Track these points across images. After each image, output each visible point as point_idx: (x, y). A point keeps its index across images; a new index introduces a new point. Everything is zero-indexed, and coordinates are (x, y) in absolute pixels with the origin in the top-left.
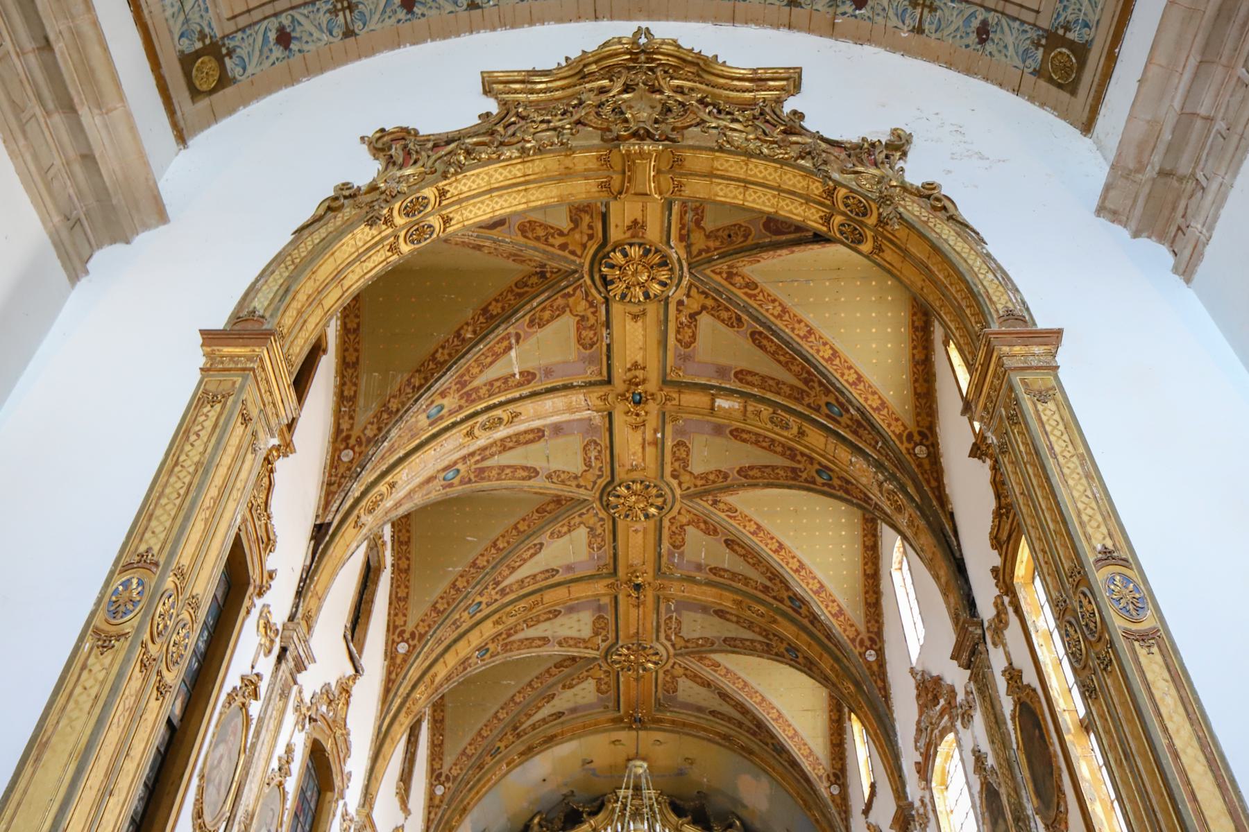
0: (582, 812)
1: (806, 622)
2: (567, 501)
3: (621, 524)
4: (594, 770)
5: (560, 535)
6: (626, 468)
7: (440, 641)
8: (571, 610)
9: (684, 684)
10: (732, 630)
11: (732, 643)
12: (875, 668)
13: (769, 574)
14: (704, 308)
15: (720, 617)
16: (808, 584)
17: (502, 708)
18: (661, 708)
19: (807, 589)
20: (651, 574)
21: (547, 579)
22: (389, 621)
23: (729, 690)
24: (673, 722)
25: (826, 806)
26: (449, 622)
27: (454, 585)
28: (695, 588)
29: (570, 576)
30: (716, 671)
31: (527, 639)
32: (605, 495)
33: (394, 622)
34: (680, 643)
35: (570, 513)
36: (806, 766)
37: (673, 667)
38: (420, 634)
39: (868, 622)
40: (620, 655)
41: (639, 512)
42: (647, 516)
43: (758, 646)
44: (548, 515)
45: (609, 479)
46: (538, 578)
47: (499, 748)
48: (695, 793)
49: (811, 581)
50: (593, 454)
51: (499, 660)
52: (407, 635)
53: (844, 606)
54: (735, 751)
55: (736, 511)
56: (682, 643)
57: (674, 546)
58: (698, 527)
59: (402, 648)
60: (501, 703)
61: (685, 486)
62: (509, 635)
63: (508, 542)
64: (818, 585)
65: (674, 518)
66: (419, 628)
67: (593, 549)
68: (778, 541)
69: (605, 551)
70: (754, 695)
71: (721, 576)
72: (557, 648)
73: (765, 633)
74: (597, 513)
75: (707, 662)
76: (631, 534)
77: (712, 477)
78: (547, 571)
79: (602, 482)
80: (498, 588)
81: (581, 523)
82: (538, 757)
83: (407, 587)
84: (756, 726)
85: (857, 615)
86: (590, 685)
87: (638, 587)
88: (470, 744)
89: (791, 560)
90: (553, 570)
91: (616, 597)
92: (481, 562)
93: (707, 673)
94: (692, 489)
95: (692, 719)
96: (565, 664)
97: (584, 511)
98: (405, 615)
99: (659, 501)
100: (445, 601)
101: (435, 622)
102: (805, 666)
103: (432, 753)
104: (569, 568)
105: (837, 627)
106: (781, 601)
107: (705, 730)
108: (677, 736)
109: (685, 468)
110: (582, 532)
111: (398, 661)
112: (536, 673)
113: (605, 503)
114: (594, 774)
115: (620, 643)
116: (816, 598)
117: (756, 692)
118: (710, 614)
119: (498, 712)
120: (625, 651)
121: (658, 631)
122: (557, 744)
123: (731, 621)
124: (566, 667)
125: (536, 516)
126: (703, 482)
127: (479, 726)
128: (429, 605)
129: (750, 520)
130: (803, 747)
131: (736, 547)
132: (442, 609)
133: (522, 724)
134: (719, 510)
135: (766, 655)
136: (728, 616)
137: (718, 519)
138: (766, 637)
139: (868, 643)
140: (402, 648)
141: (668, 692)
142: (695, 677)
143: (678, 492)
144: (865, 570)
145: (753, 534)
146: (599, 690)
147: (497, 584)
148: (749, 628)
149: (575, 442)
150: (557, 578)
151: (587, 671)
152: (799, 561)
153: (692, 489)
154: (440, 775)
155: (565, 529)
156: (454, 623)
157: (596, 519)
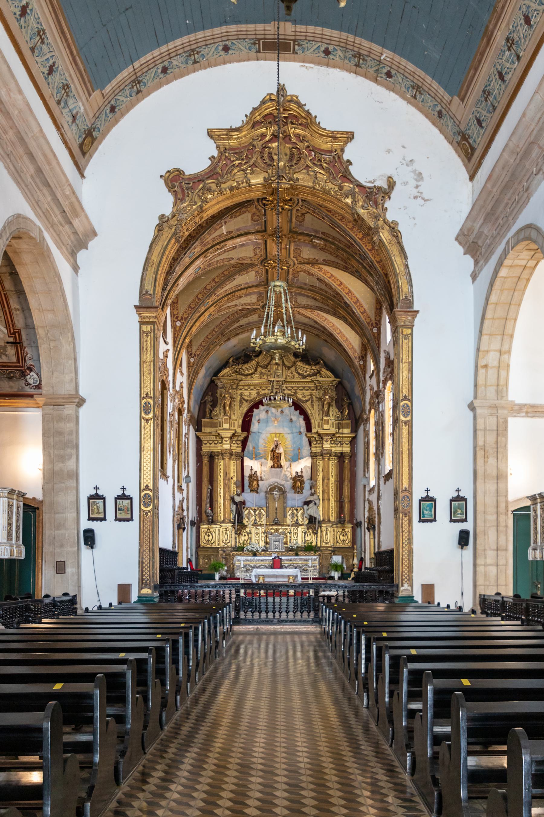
5: (243, 275)
10: (320, 305)
12: (376, 335)
14: (308, 212)
27: (197, 297)
50: (258, 251)
60: (216, 325)
85: (371, 312)
92: (209, 287)
105: (362, 318)
111: (177, 329)
125: (232, 269)
140: (178, 324)
143: (296, 262)
150: (241, 287)
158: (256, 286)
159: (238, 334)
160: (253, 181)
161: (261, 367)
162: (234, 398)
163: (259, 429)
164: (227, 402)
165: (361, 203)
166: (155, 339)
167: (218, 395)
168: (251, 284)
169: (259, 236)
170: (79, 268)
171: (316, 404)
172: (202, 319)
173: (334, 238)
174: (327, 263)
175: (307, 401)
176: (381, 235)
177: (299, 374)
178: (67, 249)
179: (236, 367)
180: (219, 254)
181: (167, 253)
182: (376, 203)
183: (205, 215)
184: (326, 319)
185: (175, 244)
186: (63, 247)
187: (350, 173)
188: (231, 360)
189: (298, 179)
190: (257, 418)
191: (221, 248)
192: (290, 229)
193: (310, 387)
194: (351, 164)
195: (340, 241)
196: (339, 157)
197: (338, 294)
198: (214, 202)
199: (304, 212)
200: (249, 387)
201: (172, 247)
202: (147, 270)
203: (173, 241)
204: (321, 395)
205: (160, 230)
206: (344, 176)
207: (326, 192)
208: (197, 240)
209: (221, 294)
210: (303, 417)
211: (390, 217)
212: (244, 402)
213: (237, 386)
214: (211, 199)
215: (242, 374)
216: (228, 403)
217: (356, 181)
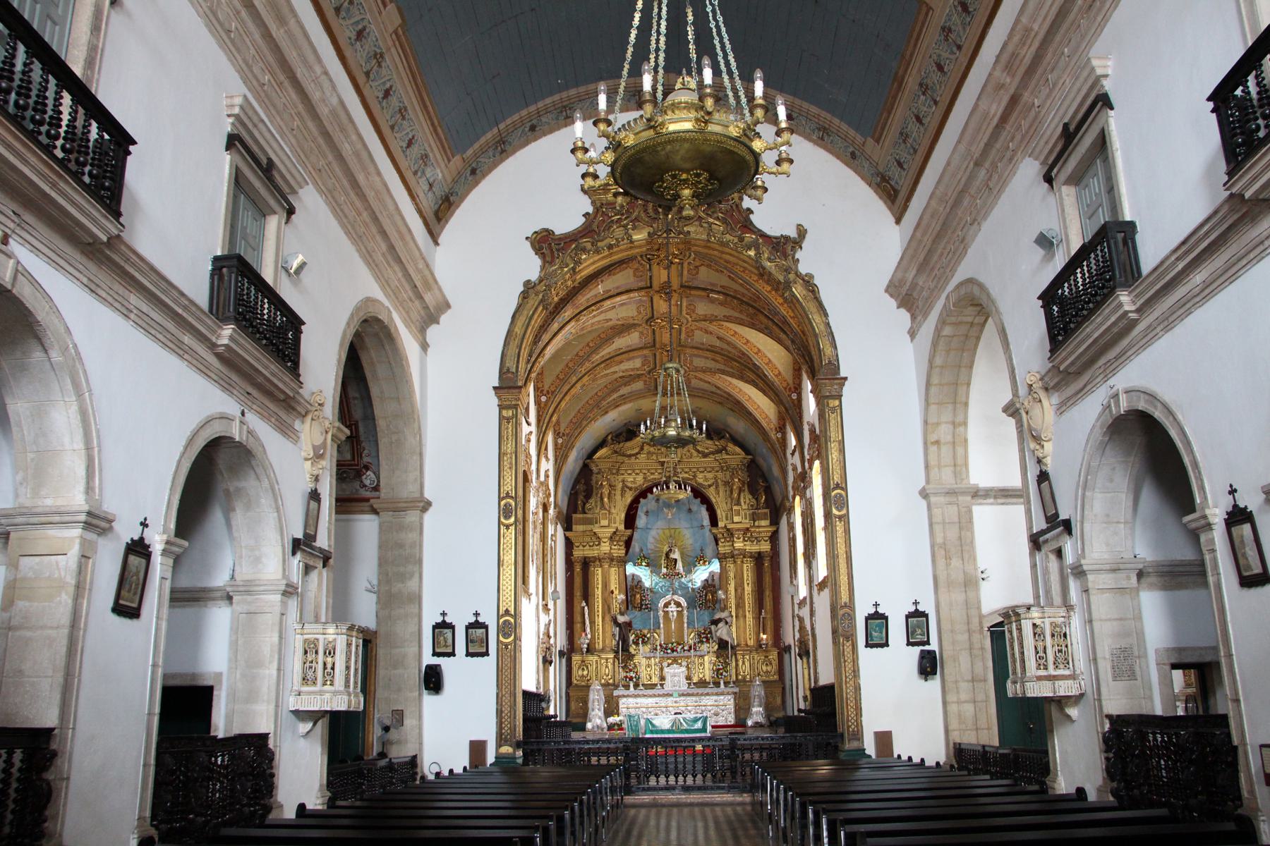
5: (623, 337)
10: (723, 367)
14: (702, 265)
27: (567, 365)
34: (691, 367)
36: (764, 424)
52: (545, 392)
59: (543, 399)
60: (590, 395)
139: (793, 390)
140: (543, 399)
149: (634, 307)
150: (622, 351)
158: (641, 348)
159: (618, 406)
160: (635, 237)
162: (614, 486)
164: (606, 491)
165: (766, 256)
166: (517, 426)
167: (593, 482)
168: (633, 348)
169: (643, 293)
170: (429, 346)
171: (721, 489)
172: (573, 391)
173: (736, 291)
174: (728, 319)
175: (710, 486)
176: (794, 290)
177: (698, 451)
178: (416, 328)
179: (617, 447)
180: (594, 316)
181: (533, 322)
182: (785, 256)
183: (578, 277)
184: (731, 383)
185: (543, 310)
186: (412, 325)
187: (751, 223)
188: (609, 437)
189: (689, 232)
190: (645, 509)
191: (597, 309)
192: (682, 282)
193: (713, 468)
194: (752, 212)
195: (743, 295)
196: (737, 206)
197: (744, 354)
198: (588, 262)
199: (698, 264)
200: (634, 471)
201: (539, 316)
202: (509, 344)
203: (541, 308)
204: (728, 477)
205: (524, 298)
206: (745, 227)
207: (723, 244)
208: (568, 302)
209: (597, 360)
210: (705, 506)
211: (803, 269)
212: (628, 490)
213: (618, 470)
214: (585, 259)
215: (624, 455)
216: (606, 493)
217: (760, 230)
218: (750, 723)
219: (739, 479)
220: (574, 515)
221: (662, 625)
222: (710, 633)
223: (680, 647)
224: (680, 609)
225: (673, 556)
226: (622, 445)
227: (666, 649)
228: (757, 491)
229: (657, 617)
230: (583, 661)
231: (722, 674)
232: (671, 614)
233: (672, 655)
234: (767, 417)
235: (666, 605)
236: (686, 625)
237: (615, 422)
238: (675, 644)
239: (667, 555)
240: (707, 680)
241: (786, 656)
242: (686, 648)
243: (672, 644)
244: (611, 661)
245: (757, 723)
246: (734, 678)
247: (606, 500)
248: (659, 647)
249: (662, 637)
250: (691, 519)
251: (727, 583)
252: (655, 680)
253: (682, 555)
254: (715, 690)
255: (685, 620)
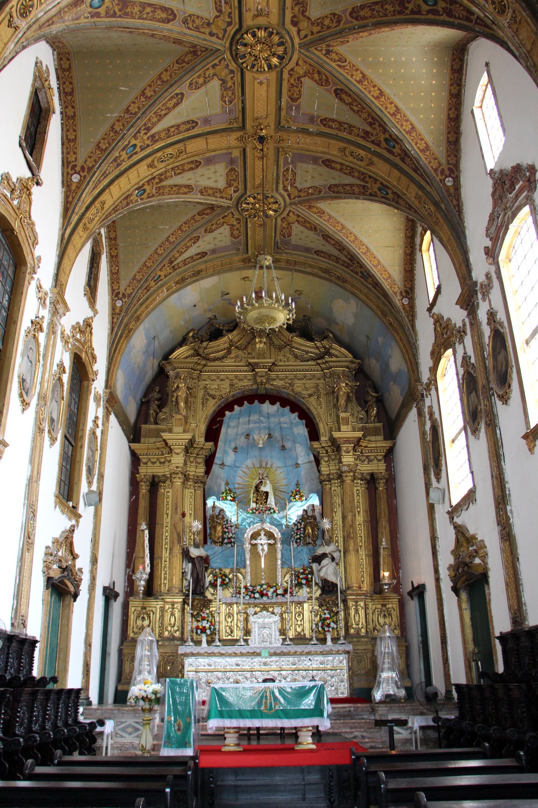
0: (222, 330)
1: (397, 160)
2: (202, 51)
3: (248, 76)
4: (230, 300)
6: (252, 14)
7: (105, 175)
8: (209, 161)
9: (296, 229)
11: (336, 189)
13: (370, 120)
15: (327, 166)
16: (402, 125)
17: (161, 246)
18: (279, 250)
19: (401, 130)
20: (273, 126)
21: (188, 130)
22: (63, 158)
23: (330, 232)
24: (287, 261)
25: (399, 312)
26: (111, 158)
27: (112, 128)
28: (309, 140)
29: (207, 129)
30: (321, 217)
31: (176, 186)
32: (234, 43)
33: (67, 158)
35: (204, 63)
36: (386, 285)
37: (288, 215)
38: (88, 167)
39: (449, 156)
40: (248, 204)
41: (263, 62)
42: (270, 67)
43: (356, 189)
44: (187, 66)
45: (237, 27)
46: (182, 128)
47: (160, 276)
48: (302, 317)
49: (404, 123)
51: (154, 202)
52: (78, 169)
53: (430, 144)
54: (331, 281)
55: (346, 61)
56: (296, 193)
57: (292, 99)
58: (312, 78)
59: (76, 178)
60: (160, 242)
61: (303, 33)
62: (161, 181)
63: (154, 91)
64: (410, 127)
65: (292, 70)
66: (87, 163)
67: (225, 102)
68: (379, 89)
69: (235, 105)
70: (349, 235)
71: (330, 127)
72: (199, 196)
73: (363, 177)
74: (228, 65)
75: (314, 210)
76: (257, 86)
77: (327, 22)
78: (188, 122)
79: (231, 30)
80: (149, 134)
81: (215, 75)
82: (189, 288)
83: (75, 131)
84: (350, 259)
86: (225, 230)
87: (262, 140)
88: (139, 272)
89: (389, 106)
90: (193, 121)
91: (244, 150)
93: (315, 218)
94: (309, 37)
95: (303, 258)
96: (206, 212)
97: (216, 62)
98: (75, 153)
99: (280, 50)
100: (106, 141)
101: (100, 158)
102: (393, 200)
103: (111, 279)
104: (207, 121)
106: (378, 145)
107: (311, 266)
108: (289, 273)
109: (303, 12)
110: (215, 83)
111: (73, 188)
112: (184, 219)
113: (234, 53)
114: (230, 304)
115: (248, 193)
116: (407, 136)
117: (351, 233)
118: (320, 165)
119: (157, 249)
120: (251, 200)
121: (277, 183)
122: (202, 278)
123: (336, 170)
124: (207, 215)
125: (176, 66)
126: (319, 28)
127: (144, 259)
128: (94, 145)
129: (357, 70)
130: (383, 273)
131: (344, 96)
132: (104, 148)
133: (176, 259)
134: (331, 59)
135: (361, 197)
136: (334, 165)
137: (329, 68)
138: (363, 180)
139: (447, 172)
140: (76, 178)
141: (284, 237)
142: (305, 223)
143: (297, 41)
144: (449, 115)
145: (359, 82)
146: (232, 235)
147: (148, 129)
148: (350, 174)
151: (223, 218)
152: (396, 106)
153: (309, 37)
154: (119, 293)
155: (201, 81)
156: (115, 160)
157: (227, 71)
161: (236, 347)
163: (235, 461)
212: (211, 399)
218: (378, 695)
219: (347, 384)
220: (144, 426)
221: (248, 562)
222: (312, 573)
223: (272, 590)
224: (272, 542)
225: (263, 489)
226: (205, 344)
227: (253, 592)
228: (366, 402)
229: (242, 553)
230: (144, 608)
231: (329, 626)
232: (260, 547)
233: (261, 601)
234: (390, 276)
235: (255, 536)
236: (279, 562)
237: (197, 312)
238: (265, 587)
239: (257, 488)
240: (308, 636)
241: (413, 605)
242: (280, 591)
243: (261, 586)
244: (178, 606)
245: (388, 696)
246: (342, 633)
247: (182, 404)
248: (243, 590)
249: (249, 578)
250: (285, 458)
251: (332, 511)
252: (238, 634)
253: (275, 489)
254: (320, 648)
255: (279, 556)
